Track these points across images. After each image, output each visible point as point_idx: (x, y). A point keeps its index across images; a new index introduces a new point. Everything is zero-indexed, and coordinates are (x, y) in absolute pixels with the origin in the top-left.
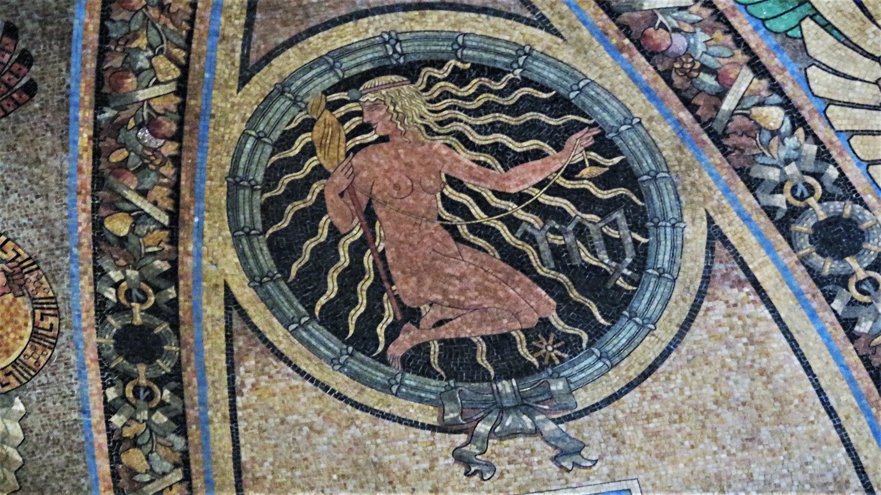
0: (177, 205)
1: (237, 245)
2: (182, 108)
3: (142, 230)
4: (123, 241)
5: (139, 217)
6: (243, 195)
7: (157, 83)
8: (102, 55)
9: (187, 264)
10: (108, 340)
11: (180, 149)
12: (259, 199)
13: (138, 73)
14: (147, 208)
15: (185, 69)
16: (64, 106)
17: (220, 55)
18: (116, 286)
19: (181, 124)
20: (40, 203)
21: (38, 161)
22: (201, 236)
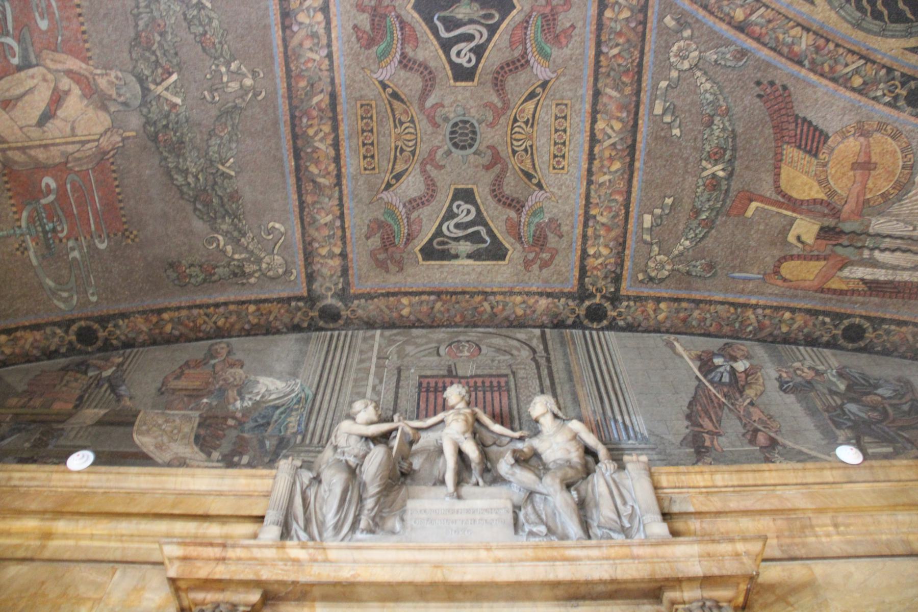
0: (858, 54)
1: (887, 37)
2: (815, 33)
3: (863, 73)
4: (865, 83)
5: (857, 71)
6: (864, 25)
7: (801, 38)
8: (780, 54)
9: (886, 61)
10: (909, 109)
11: (833, 42)
12: (869, 18)
13: (793, 43)
14: (854, 66)
15: (798, 25)
16: (797, 79)
17: (798, 8)
18: (884, 95)
19: (822, 37)
20: (835, 108)
21: (816, 100)
22: (876, 50)
